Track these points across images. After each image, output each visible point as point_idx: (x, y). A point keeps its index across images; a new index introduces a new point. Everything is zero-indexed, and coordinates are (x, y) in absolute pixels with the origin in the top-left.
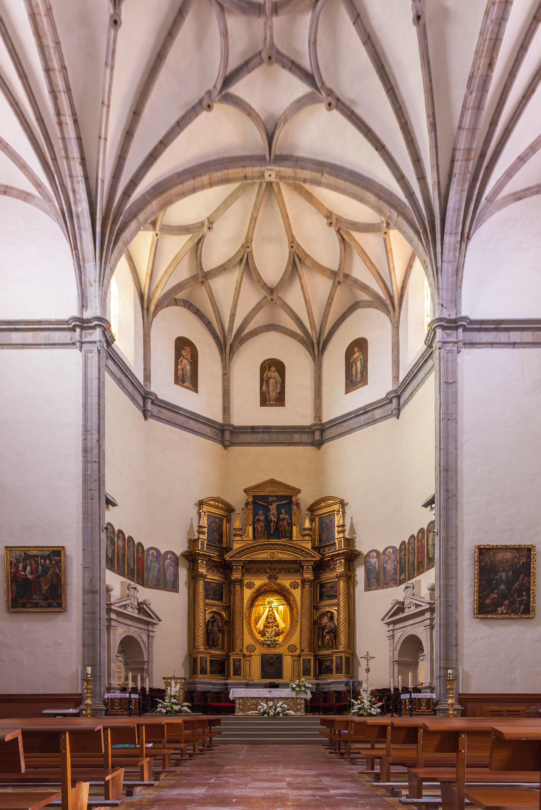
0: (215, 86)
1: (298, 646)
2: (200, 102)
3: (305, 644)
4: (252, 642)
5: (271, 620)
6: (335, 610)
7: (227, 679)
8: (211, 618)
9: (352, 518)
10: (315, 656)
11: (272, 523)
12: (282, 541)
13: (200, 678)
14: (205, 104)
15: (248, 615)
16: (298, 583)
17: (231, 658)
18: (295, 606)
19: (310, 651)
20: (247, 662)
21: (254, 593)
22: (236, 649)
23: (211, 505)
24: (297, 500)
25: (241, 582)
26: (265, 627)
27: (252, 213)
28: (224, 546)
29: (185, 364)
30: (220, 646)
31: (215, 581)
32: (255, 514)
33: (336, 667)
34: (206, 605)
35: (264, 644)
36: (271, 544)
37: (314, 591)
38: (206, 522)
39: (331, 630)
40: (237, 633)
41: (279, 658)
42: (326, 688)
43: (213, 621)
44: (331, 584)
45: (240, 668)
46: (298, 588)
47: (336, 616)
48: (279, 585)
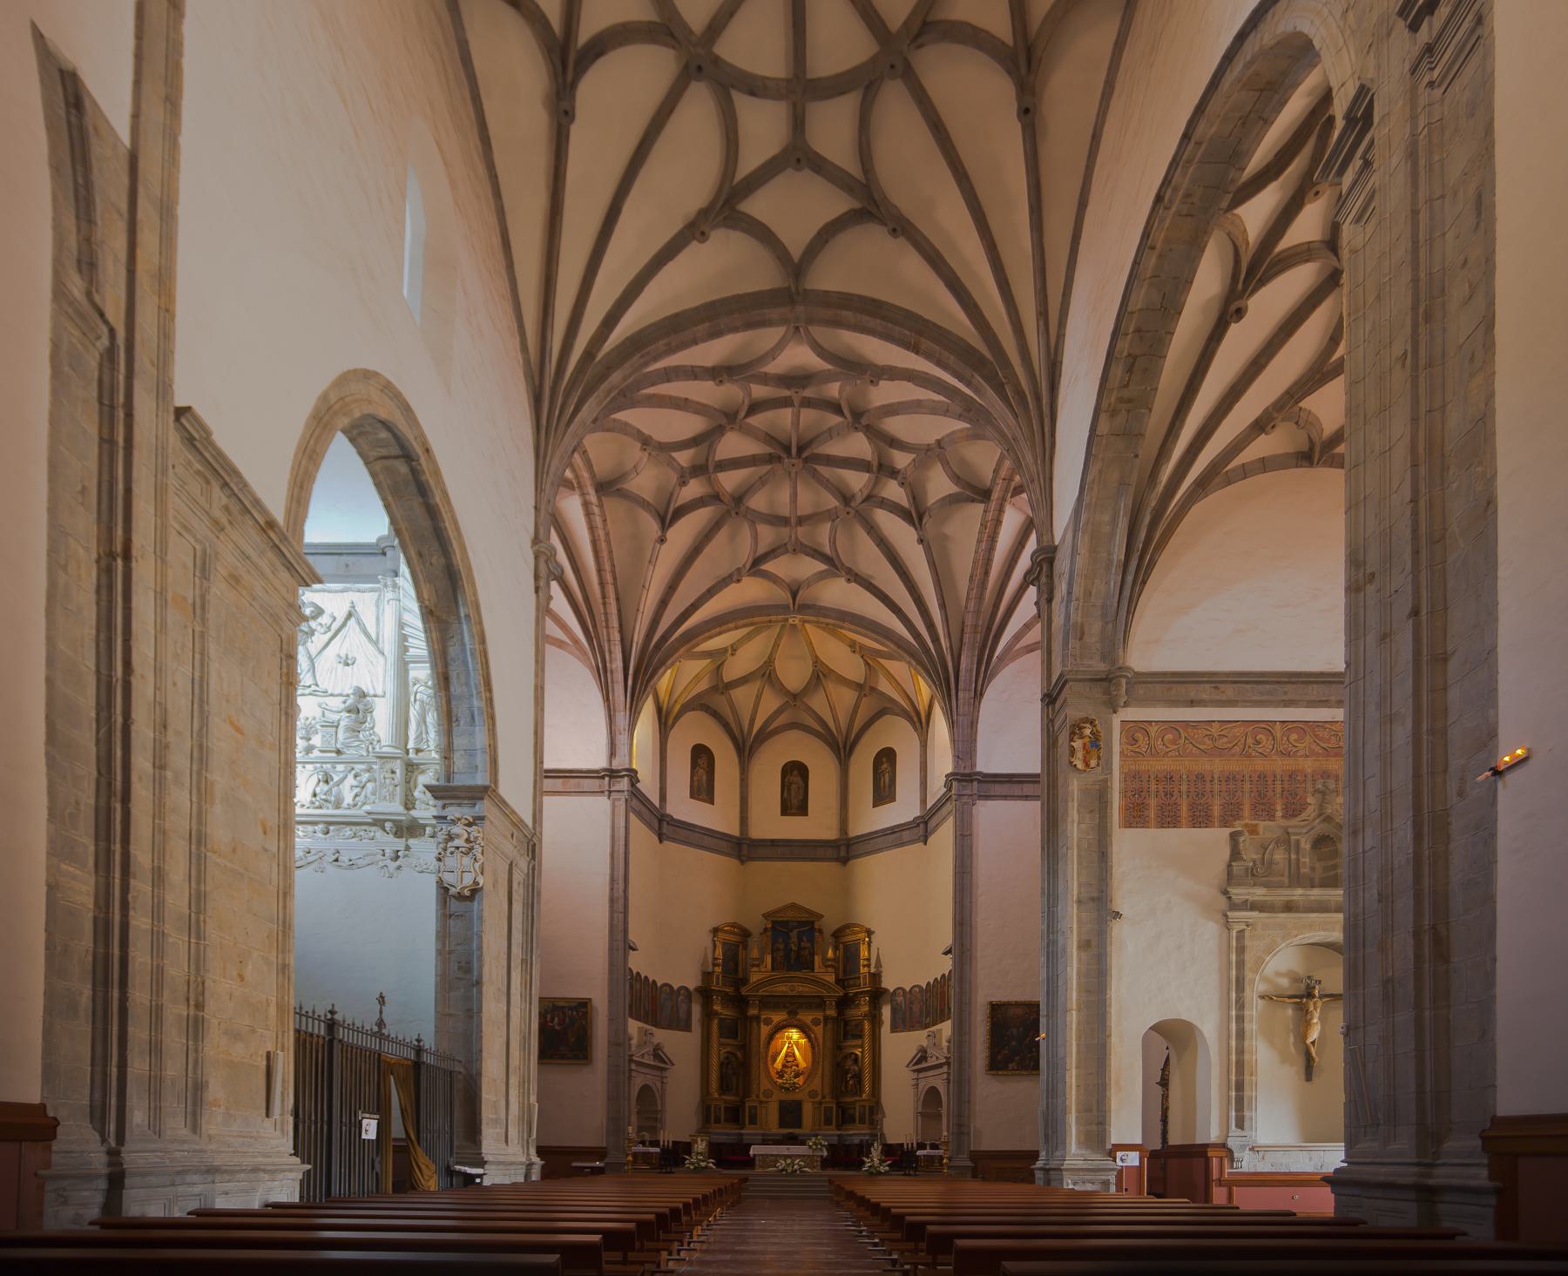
0: (744, 566)
2: (731, 576)
3: (827, 1091)
14: (735, 578)
23: (726, 932)
25: (757, 1018)
26: (784, 1066)
32: (774, 942)
35: (782, 1088)
41: (798, 1105)
48: (800, 1021)
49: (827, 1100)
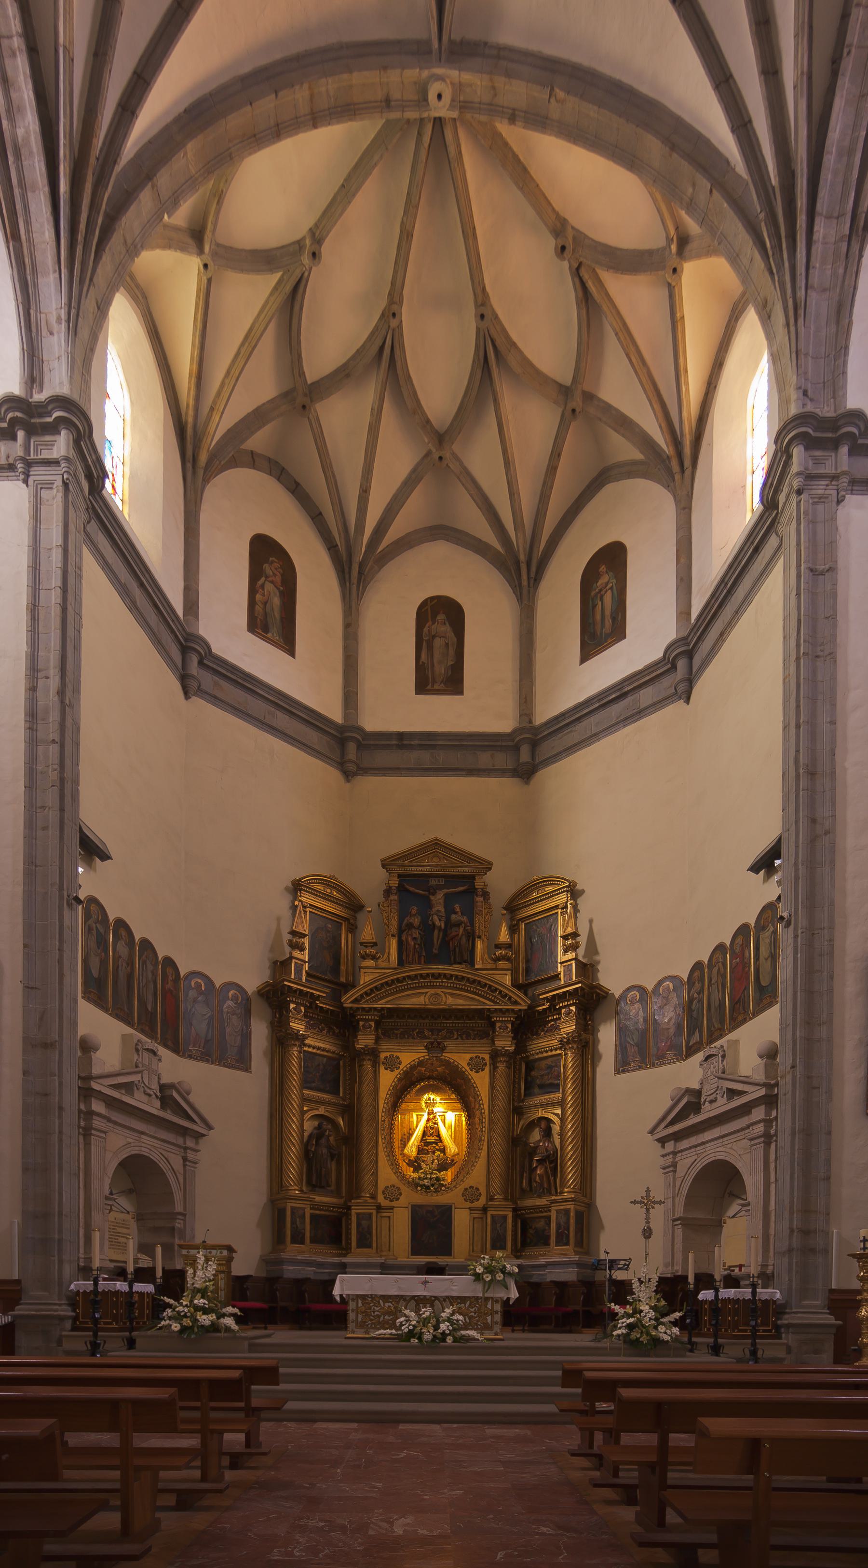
1: (483, 1190)
4: (394, 1180)
5: (431, 1134)
6: (556, 1115)
7: (345, 1255)
8: (315, 1128)
9: (591, 921)
10: (515, 1210)
11: (436, 932)
12: (456, 969)
13: (292, 1251)
15: (387, 1123)
16: (483, 1059)
17: (353, 1212)
18: (477, 1107)
19: (506, 1199)
20: (385, 1222)
21: (400, 1080)
22: (363, 1194)
24: (486, 885)
25: (374, 1054)
27: (402, 222)
28: (343, 979)
29: (269, 593)
30: (333, 1188)
31: (325, 1053)
33: (557, 1231)
34: (305, 1100)
35: (417, 1185)
36: (433, 975)
37: (514, 1077)
38: (306, 926)
39: (548, 1156)
40: (366, 1159)
41: (446, 1212)
42: (536, 1276)
43: (318, 1135)
44: (548, 1062)
45: (370, 1233)
46: (483, 1070)
47: (556, 1128)
48: (448, 1064)
49: (496, 1203)
